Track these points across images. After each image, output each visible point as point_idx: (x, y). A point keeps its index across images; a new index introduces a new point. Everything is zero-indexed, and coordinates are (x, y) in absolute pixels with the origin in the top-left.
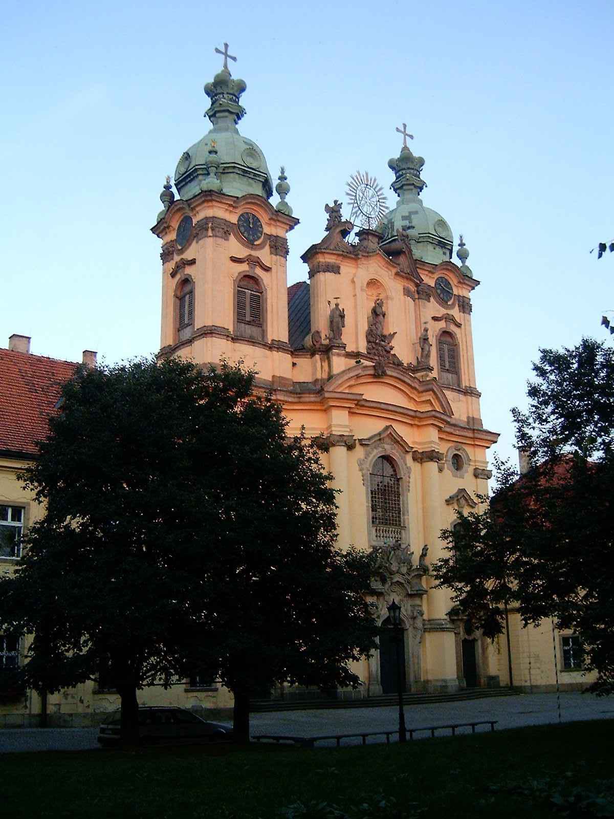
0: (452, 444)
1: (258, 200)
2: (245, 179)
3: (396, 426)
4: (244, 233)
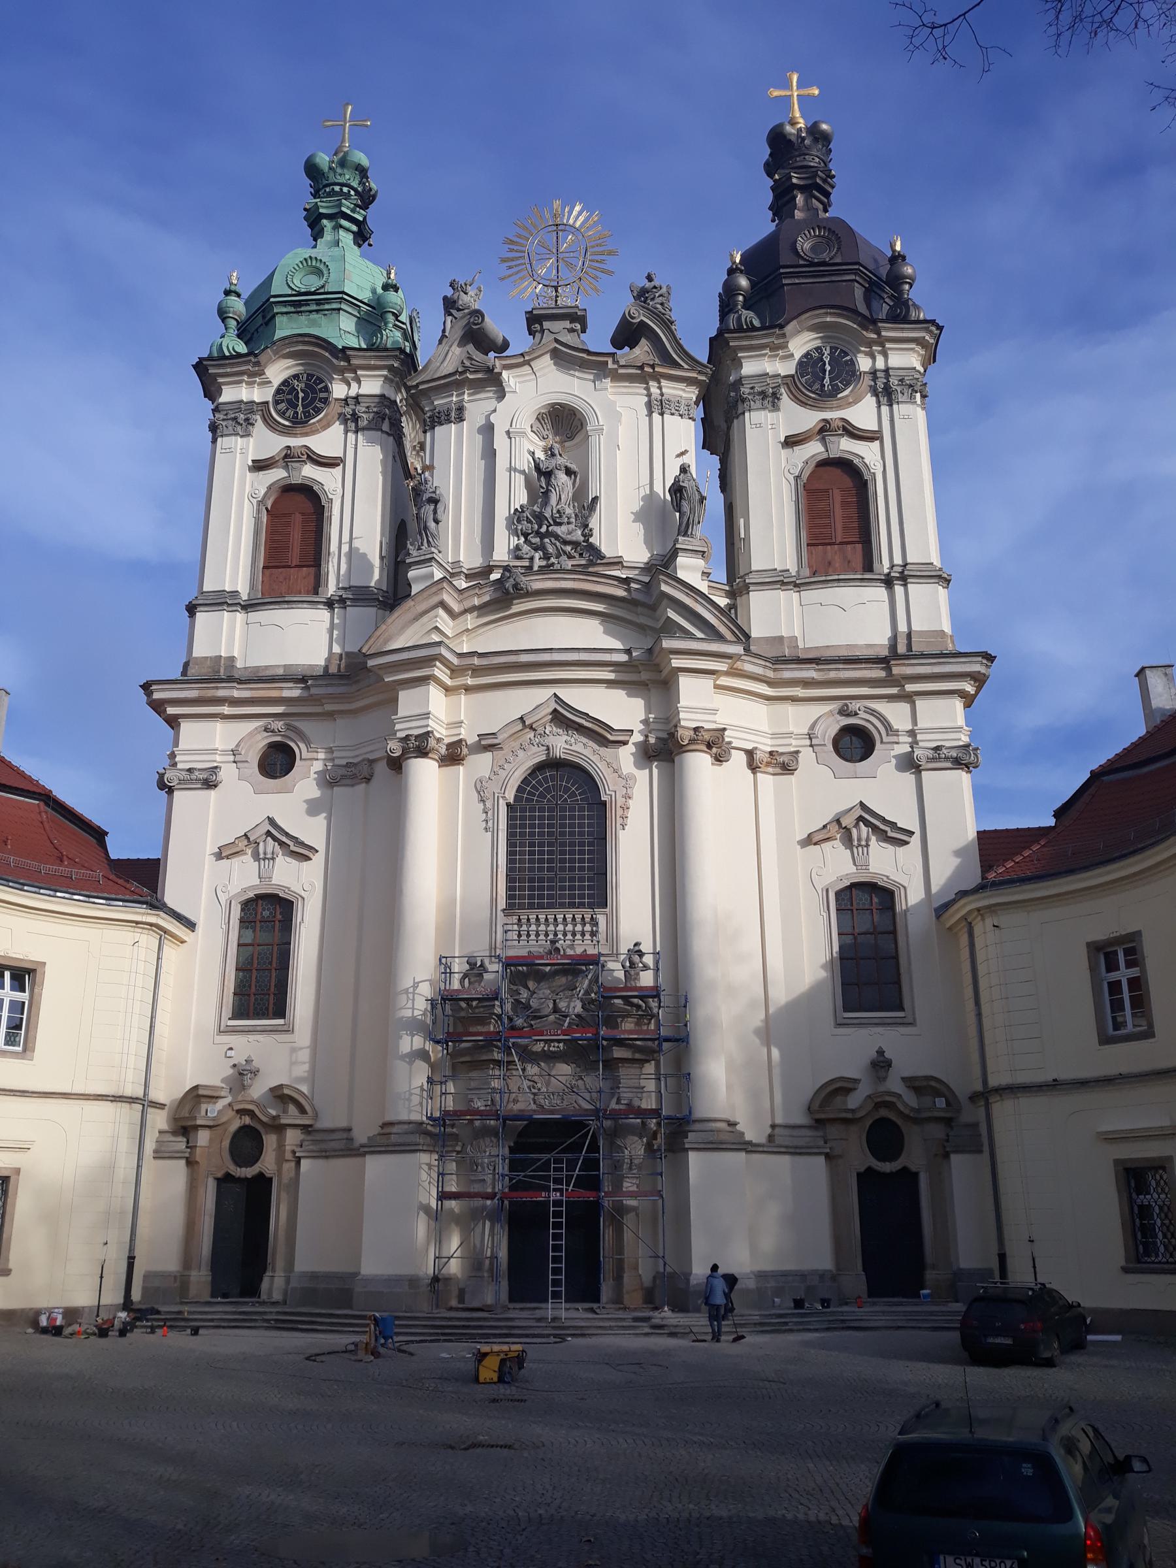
0: (834, 706)
1: (305, 343)
2: (303, 318)
3: (566, 694)
4: (284, 413)
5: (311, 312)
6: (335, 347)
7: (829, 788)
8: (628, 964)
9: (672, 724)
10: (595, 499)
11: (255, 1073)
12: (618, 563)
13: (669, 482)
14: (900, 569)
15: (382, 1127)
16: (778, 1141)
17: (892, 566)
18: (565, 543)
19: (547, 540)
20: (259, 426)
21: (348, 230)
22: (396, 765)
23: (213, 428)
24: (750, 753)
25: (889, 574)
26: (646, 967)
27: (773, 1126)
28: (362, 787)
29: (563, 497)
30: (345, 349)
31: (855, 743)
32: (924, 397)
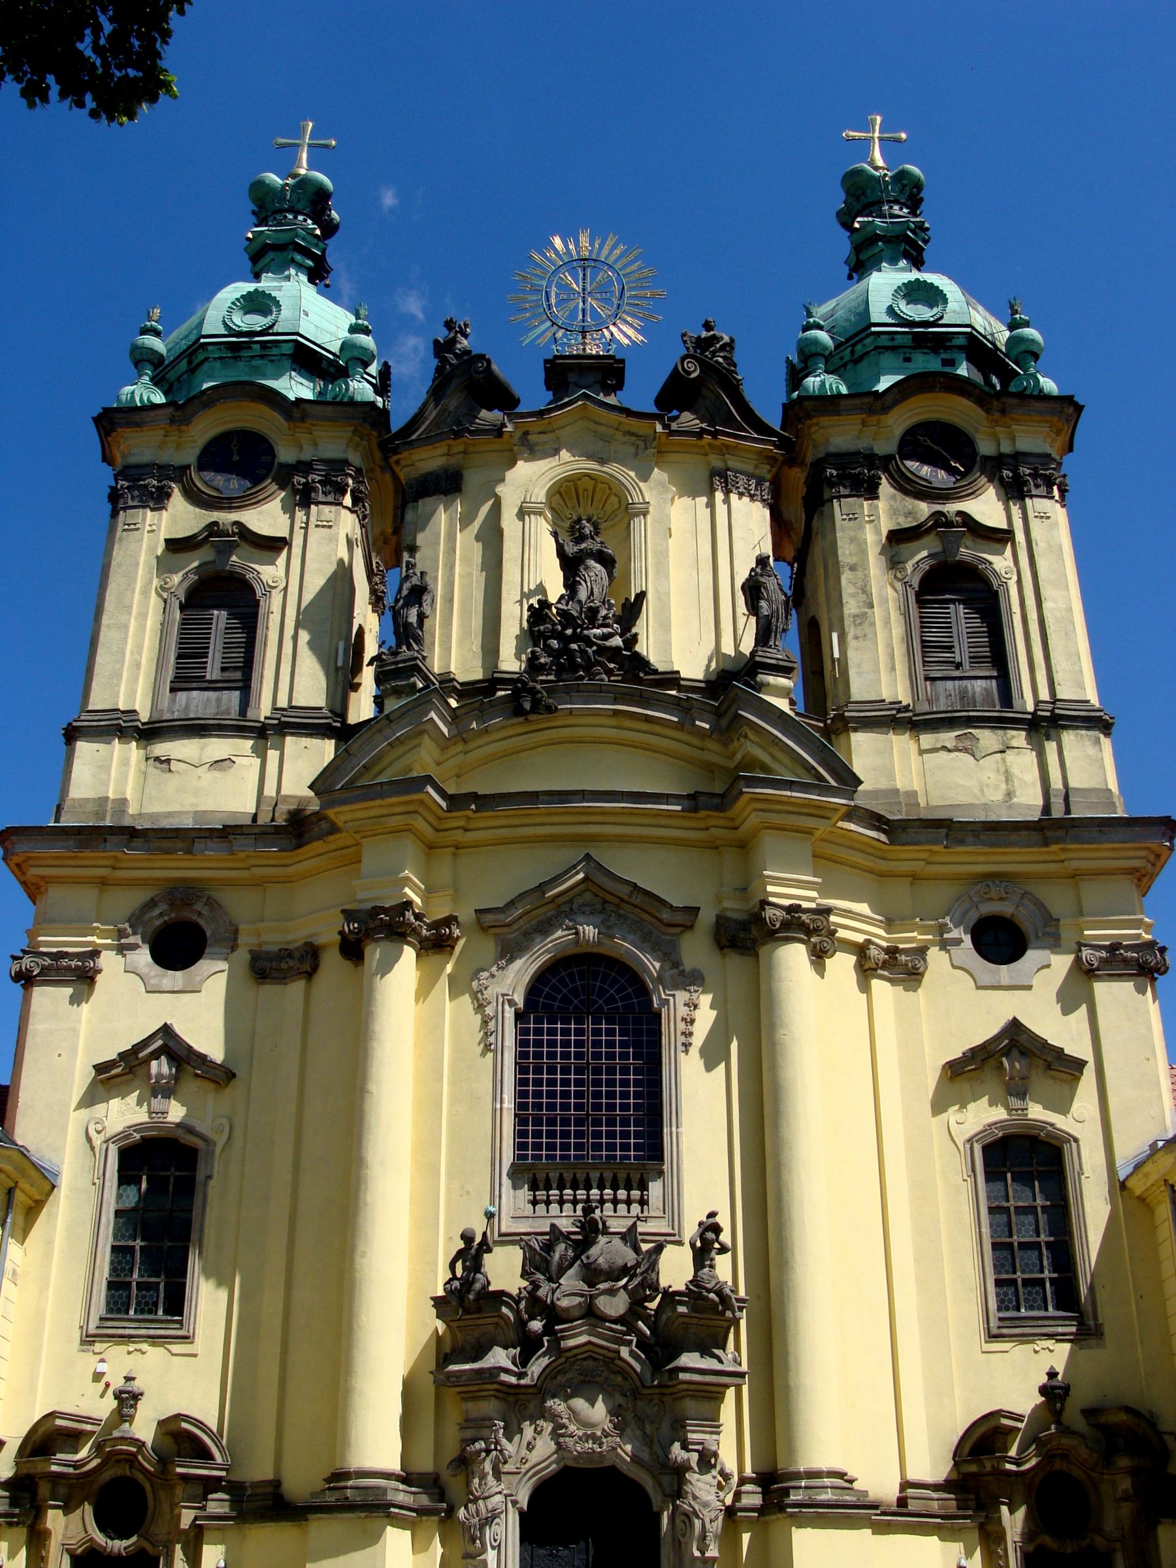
5: (252, 357)
6: (285, 398)
7: (962, 1003)
8: (698, 1244)
9: (755, 901)
10: (641, 596)
11: (136, 1397)
12: (672, 679)
13: (742, 576)
14: (1050, 707)
15: (328, 1480)
16: (913, 1506)
17: (1037, 702)
18: (602, 650)
19: (574, 646)
20: (177, 501)
21: (300, 267)
22: (352, 950)
23: (115, 497)
24: (861, 950)
25: (1034, 714)
26: (723, 1250)
27: (906, 1485)
28: (299, 986)
29: (596, 590)
30: (299, 401)
31: (1000, 941)
32: (1062, 492)
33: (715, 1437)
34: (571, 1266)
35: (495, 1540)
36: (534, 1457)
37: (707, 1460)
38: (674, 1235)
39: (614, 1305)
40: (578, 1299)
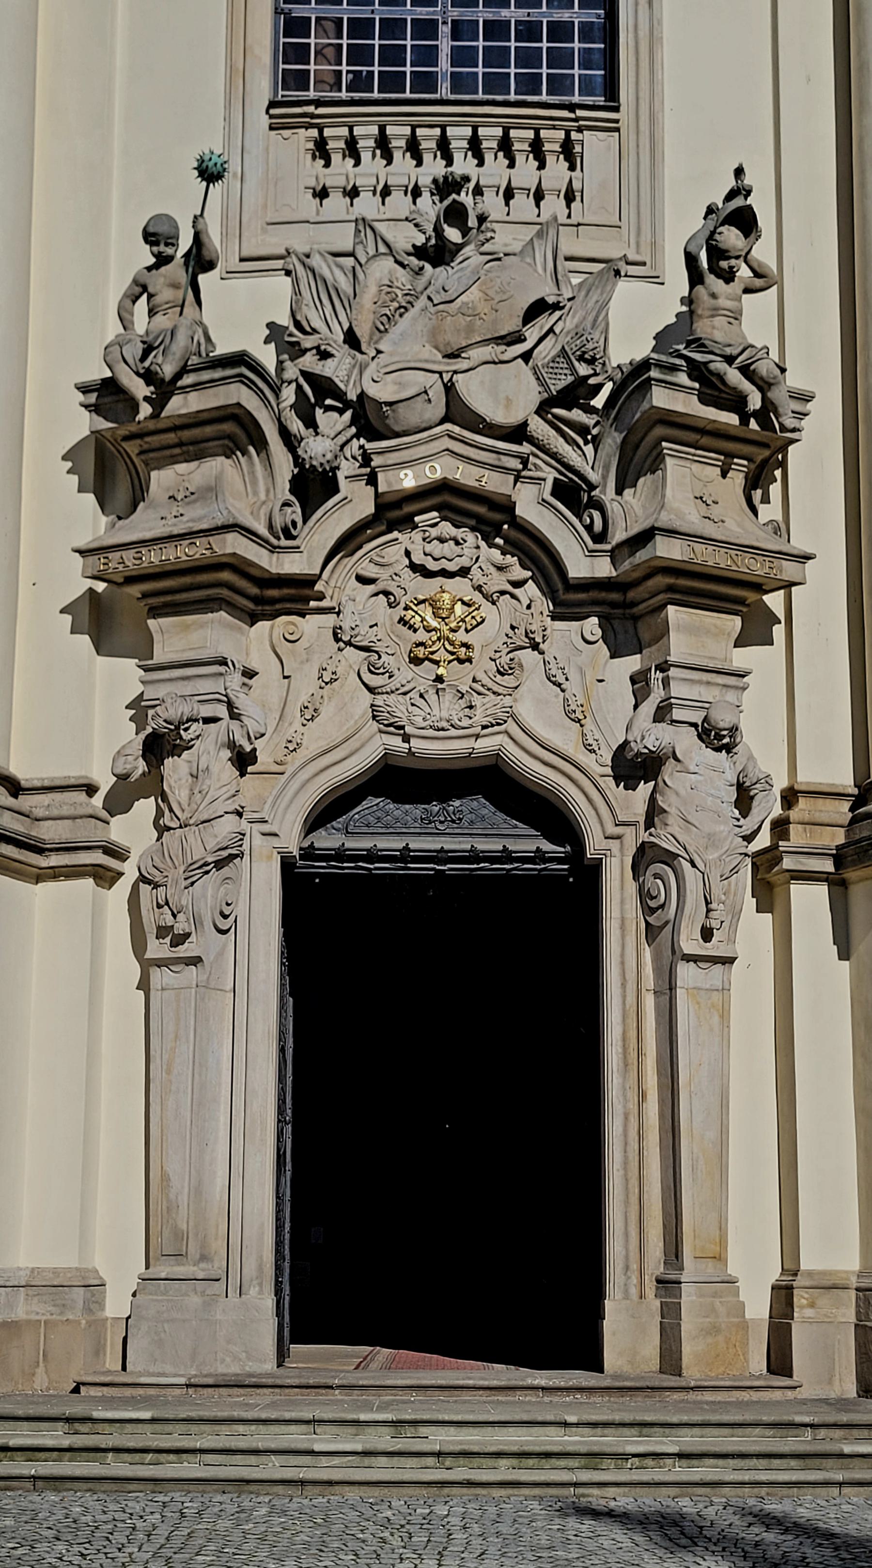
33: (731, 696)
34: (403, 309)
35: (225, 917)
36: (314, 738)
37: (717, 738)
38: (644, 264)
39: (506, 392)
40: (421, 380)
